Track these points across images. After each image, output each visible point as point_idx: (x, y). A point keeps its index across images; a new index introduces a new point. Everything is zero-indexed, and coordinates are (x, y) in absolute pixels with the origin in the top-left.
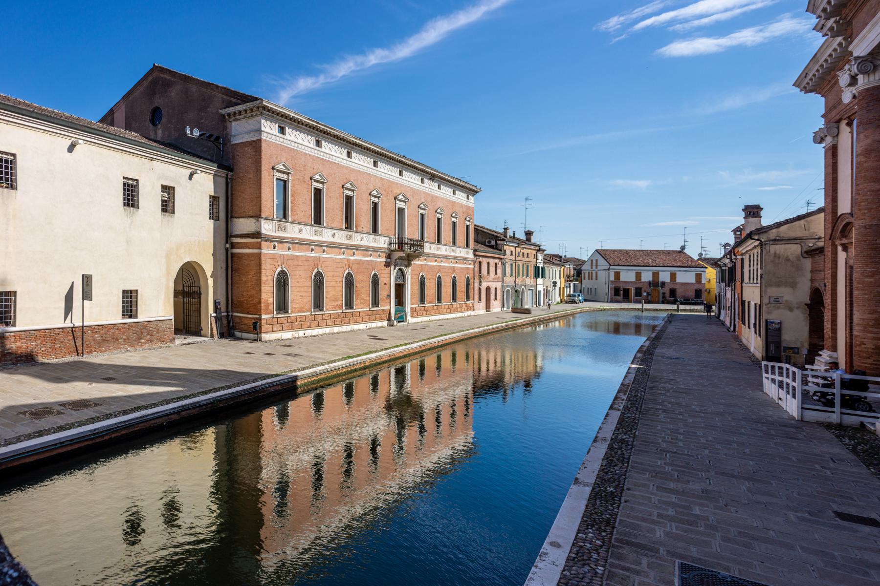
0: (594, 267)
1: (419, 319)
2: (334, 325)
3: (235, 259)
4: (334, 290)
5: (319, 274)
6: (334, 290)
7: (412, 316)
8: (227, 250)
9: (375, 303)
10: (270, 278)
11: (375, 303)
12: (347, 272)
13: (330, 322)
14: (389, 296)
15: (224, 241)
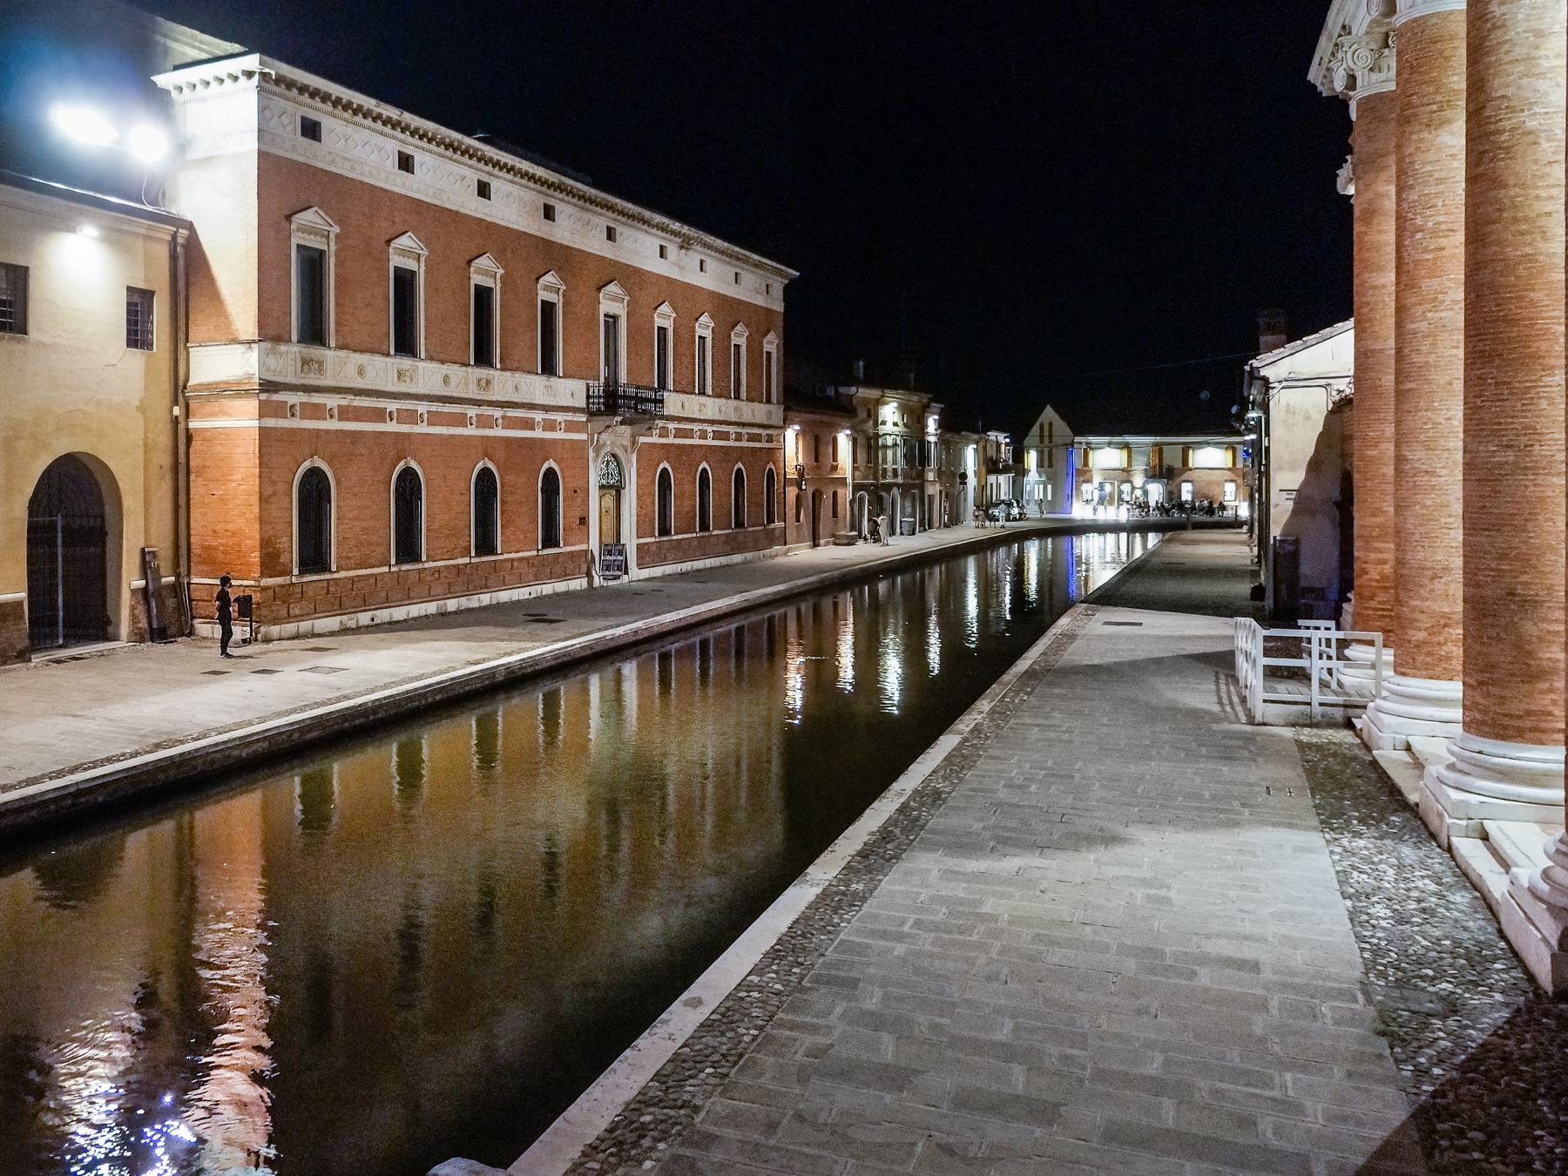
0: (1046, 440)
1: (657, 571)
2: (450, 594)
3: (196, 445)
4: (445, 509)
5: (408, 477)
6: (445, 509)
7: (641, 566)
8: (175, 421)
9: (550, 540)
10: (281, 487)
11: (550, 540)
12: (480, 466)
13: (438, 589)
14: (584, 521)
15: (167, 401)
